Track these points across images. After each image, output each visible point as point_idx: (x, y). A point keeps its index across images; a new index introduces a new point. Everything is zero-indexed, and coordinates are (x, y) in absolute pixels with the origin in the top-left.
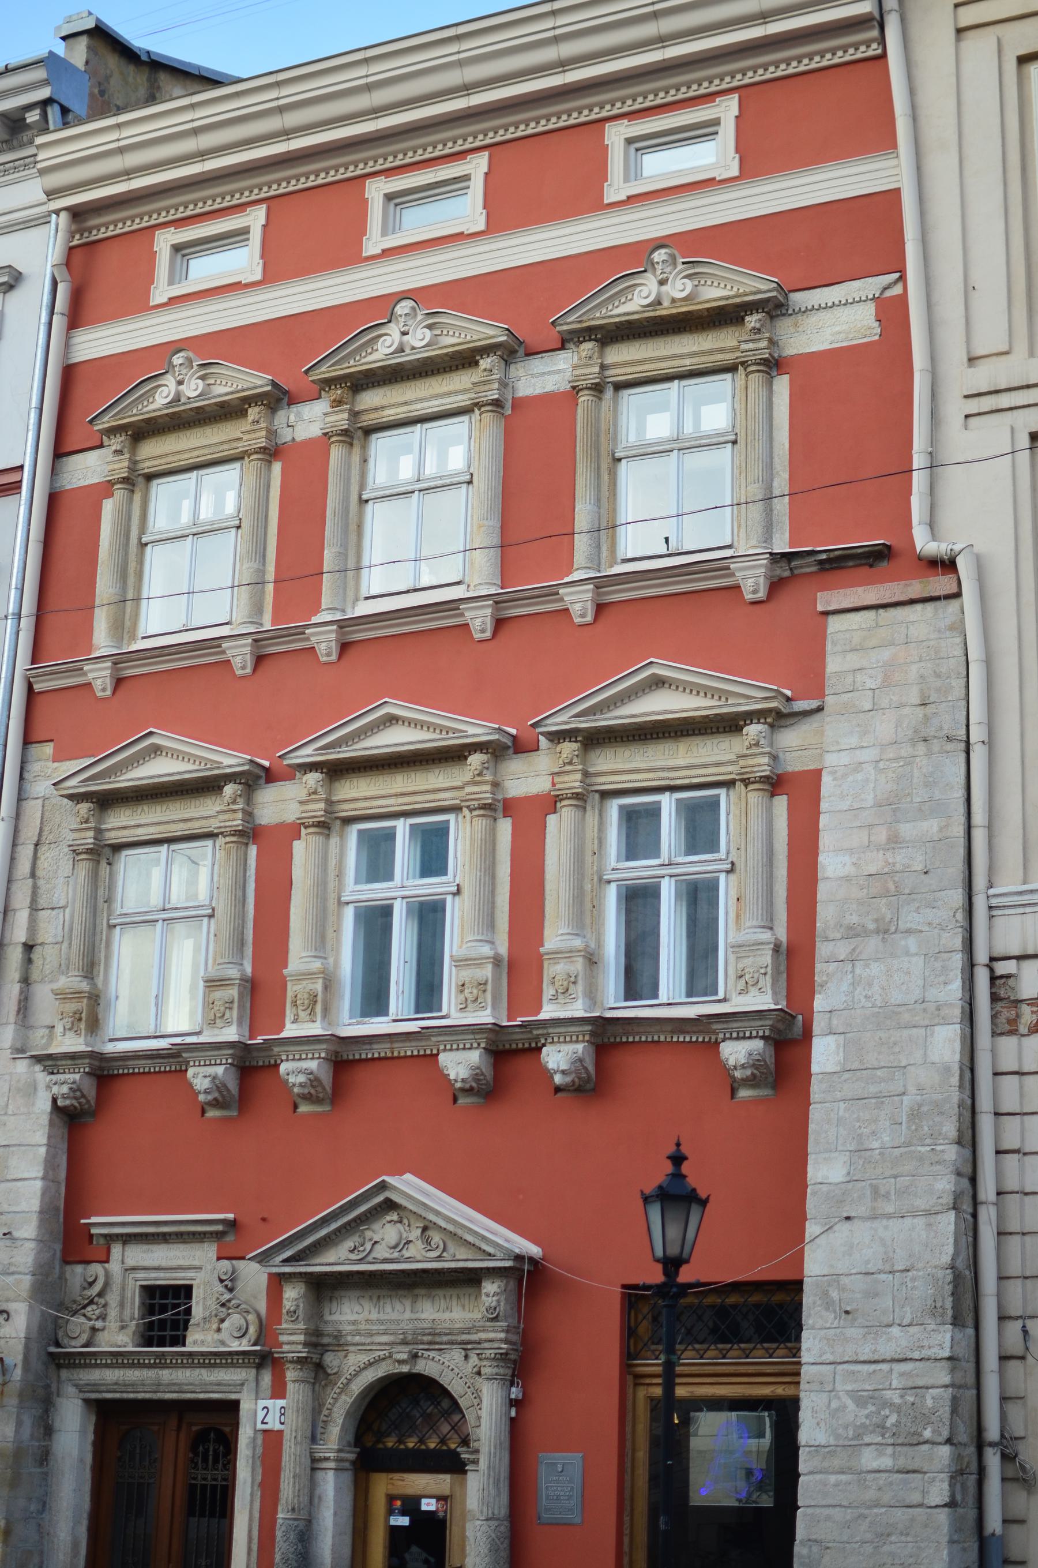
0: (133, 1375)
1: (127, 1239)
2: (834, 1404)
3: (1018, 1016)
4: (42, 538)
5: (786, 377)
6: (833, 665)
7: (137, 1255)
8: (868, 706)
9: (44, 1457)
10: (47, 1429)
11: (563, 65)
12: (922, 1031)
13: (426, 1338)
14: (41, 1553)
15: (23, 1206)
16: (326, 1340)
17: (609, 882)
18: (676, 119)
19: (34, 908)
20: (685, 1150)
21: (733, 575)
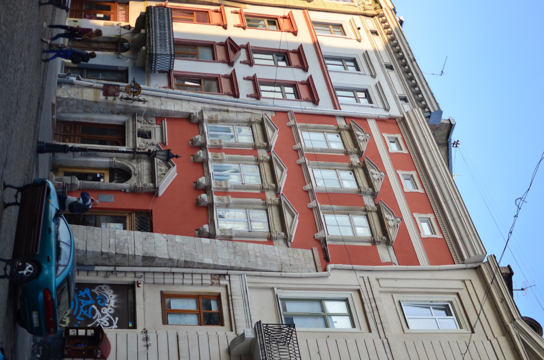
0: (131, 128)
1: (162, 128)
2: (125, 235)
3: (216, 280)
4: (324, 114)
5: (371, 245)
6: (300, 250)
7: (158, 130)
8: (289, 255)
9: (112, 113)
10: (118, 114)
11: (446, 202)
12: (211, 257)
13: (140, 177)
14: (91, 112)
15: (168, 107)
16: (139, 160)
17: (246, 210)
18: (434, 223)
19: (237, 112)
20: (179, 158)
21: (320, 231)
